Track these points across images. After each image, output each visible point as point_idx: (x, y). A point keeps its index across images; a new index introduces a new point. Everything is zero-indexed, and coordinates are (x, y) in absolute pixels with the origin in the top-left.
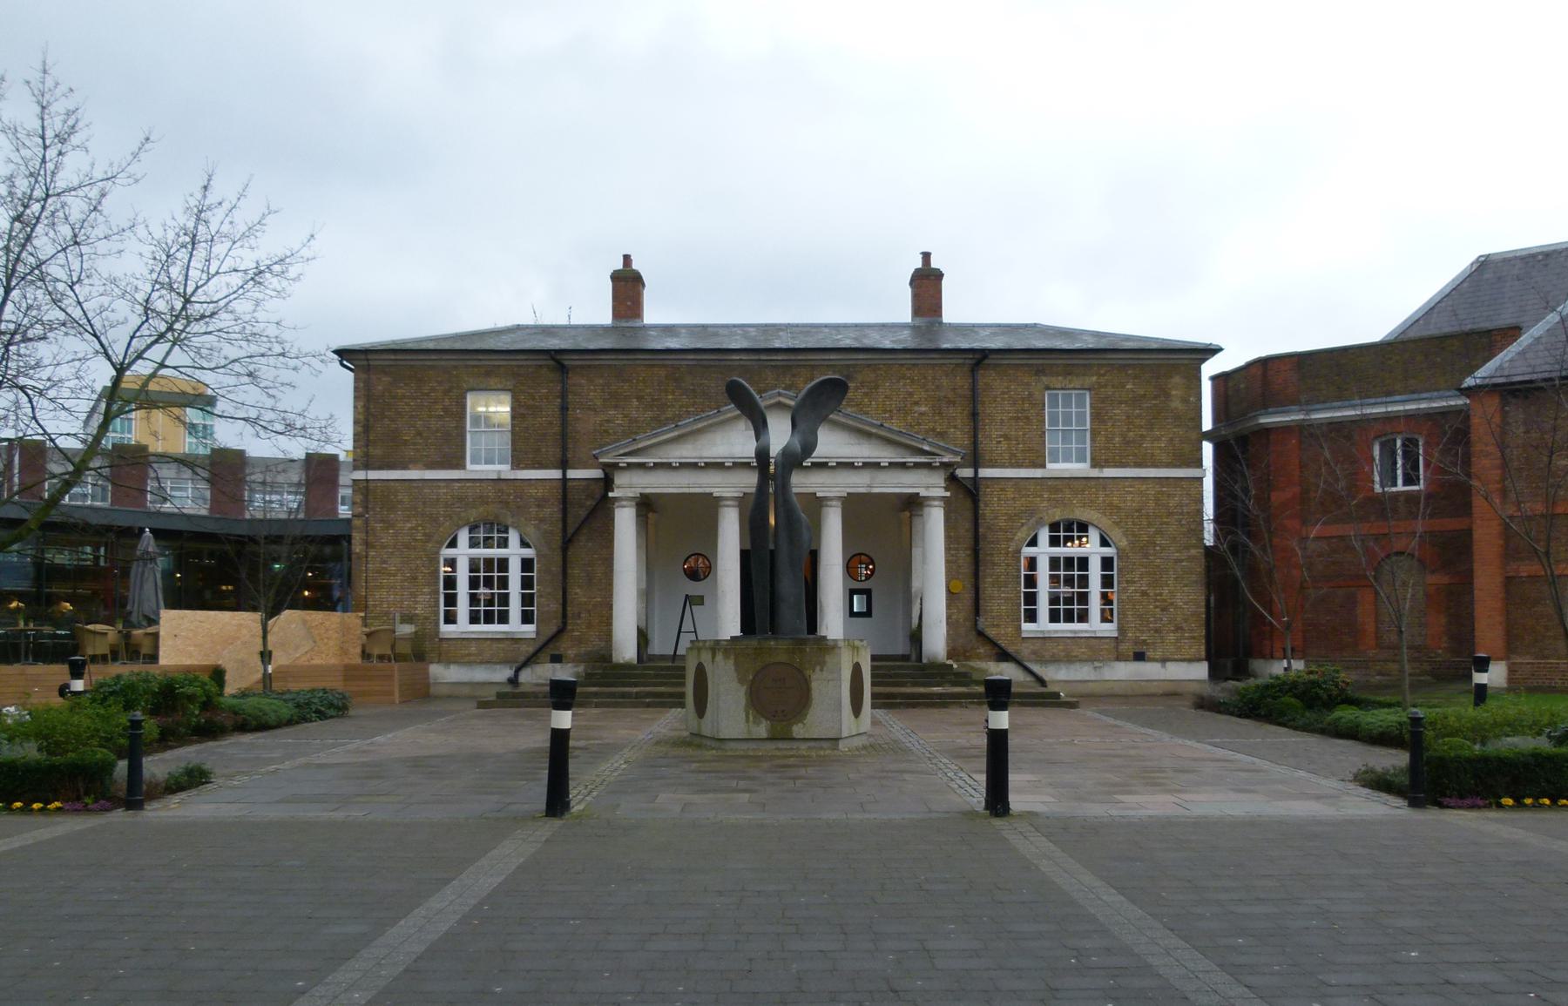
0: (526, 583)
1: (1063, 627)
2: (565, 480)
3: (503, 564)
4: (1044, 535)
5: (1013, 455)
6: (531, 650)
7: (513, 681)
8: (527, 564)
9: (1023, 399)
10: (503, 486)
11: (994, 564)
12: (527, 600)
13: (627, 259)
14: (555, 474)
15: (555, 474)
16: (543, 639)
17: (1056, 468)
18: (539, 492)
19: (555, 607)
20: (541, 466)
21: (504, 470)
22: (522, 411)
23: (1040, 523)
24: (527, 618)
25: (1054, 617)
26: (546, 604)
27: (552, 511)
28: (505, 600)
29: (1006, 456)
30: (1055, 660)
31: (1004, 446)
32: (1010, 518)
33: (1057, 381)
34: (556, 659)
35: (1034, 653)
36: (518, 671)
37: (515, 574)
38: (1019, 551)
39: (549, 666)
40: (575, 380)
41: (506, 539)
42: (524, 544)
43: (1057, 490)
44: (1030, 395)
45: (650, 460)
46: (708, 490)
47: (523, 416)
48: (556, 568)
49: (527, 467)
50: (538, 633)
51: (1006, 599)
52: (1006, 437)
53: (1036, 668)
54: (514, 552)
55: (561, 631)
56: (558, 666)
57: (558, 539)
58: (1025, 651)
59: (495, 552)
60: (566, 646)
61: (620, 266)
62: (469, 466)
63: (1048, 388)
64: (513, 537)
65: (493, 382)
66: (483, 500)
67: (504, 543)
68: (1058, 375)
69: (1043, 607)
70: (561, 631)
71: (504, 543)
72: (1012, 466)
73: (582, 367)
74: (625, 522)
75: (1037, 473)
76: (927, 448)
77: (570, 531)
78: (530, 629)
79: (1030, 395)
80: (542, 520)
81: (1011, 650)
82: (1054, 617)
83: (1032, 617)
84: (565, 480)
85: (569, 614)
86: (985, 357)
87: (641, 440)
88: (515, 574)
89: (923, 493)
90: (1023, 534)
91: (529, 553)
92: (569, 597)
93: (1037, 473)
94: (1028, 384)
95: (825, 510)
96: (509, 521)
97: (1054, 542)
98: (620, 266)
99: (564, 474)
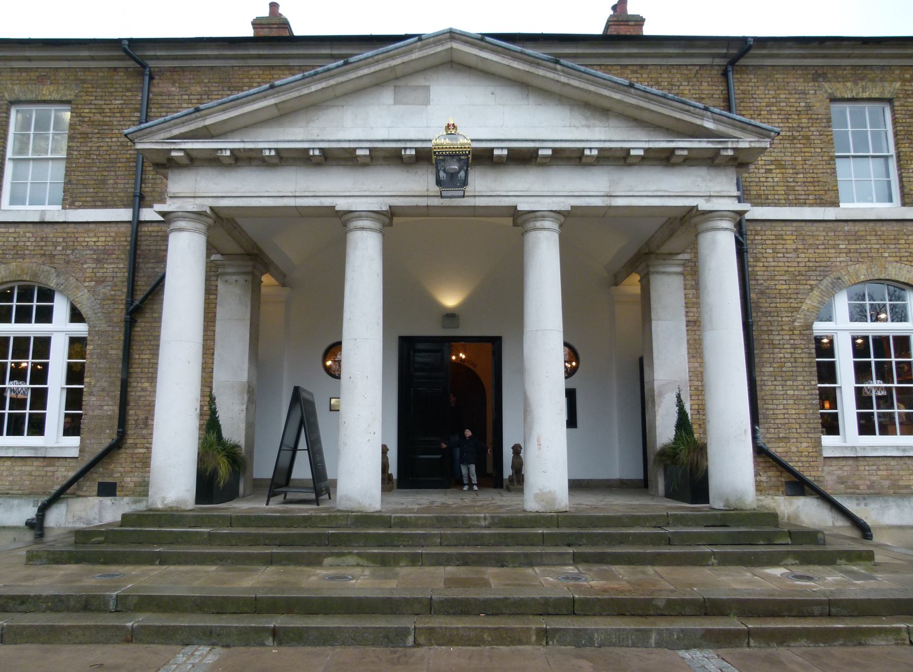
0: (74, 374)
1: (877, 441)
2: (137, 224)
3: (43, 345)
4: (842, 304)
5: (790, 189)
6: (72, 474)
7: (37, 526)
8: (77, 345)
9: (799, 113)
10: (48, 230)
11: (773, 345)
12: (74, 399)
13: (274, 6)
14: (125, 214)
15: (125, 214)
16: (88, 458)
17: (852, 207)
18: (101, 240)
19: (111, 409)
20: (105, 205)
21: (55, 212)
22: (85, 129)
23: (837, 285)
24: (72, 427)
25: (866, 427)
26: (100, 406)
27: (117, 268)
28: (40, 398)
29: (781, 190)
30: (875, 493)
31: (777, 175)
32: (796, 277)
33: (847, 89)
34: (108, 490)
35: (841, 481)
36: (43, 510)
37: (58, 362)
38: (809, 327)
39: (95, 501)
40: (162, 86)
41: (51, 309)
42: (76, 316)
43: (858, 238)
44: (809, 107)
45: (226, 146)
46: (327, 202)
47: (85, 135)
48: (116, 352)
49: (84, 206)
50: (82, 450)
51: (797, 399)
52: (779, 165)
53: (850, 505)
54: (60, 329)
55: (117, 445)
56: (107, 501)
57: (119, 313)
58: (828, 480)
59: (32, 329)
60: (120, 469)
61: (265, 12)
62: (5, 204)
63: (834, 100)
64: (60, 307)
65: (47, 91)
66: (19, 253)
67: (45, 316)
68: (845, 79)
69: (848, 411)
70: (117, 445)
71: (45, 316)
72: (791, 204)
73: (173, 70)
74: (185, 261)
75: (829, 213)
76: (710, 125)
77: (139, 296)
78: (75, 441)
79: (809, 107)
80: (100, 281)
81: (809, 475)
82: (866, 427)
83: (831, 426)
84: (137, 224)
85: (131, 421)
86: (743, 54)
87: (211, 111)
88: (58, 362)
89: (703, 205)
90: (811, 302)
91: (80, 329)
92: (133, 395)
93: (829, 213)
94: (804, 93)
95: (532, 237)
96: (52, 284)
97: (858, 314)
98: (265, 12)
99: (136, 214)
